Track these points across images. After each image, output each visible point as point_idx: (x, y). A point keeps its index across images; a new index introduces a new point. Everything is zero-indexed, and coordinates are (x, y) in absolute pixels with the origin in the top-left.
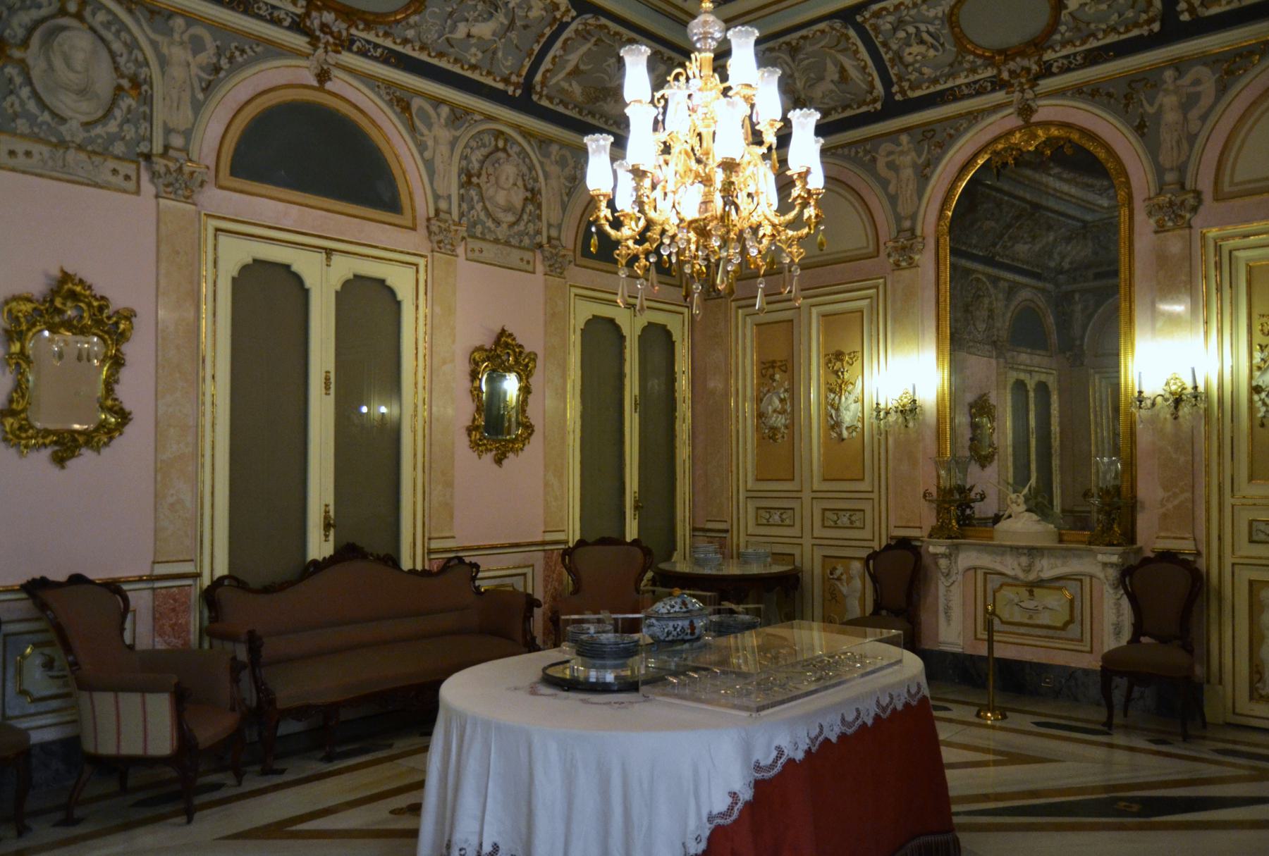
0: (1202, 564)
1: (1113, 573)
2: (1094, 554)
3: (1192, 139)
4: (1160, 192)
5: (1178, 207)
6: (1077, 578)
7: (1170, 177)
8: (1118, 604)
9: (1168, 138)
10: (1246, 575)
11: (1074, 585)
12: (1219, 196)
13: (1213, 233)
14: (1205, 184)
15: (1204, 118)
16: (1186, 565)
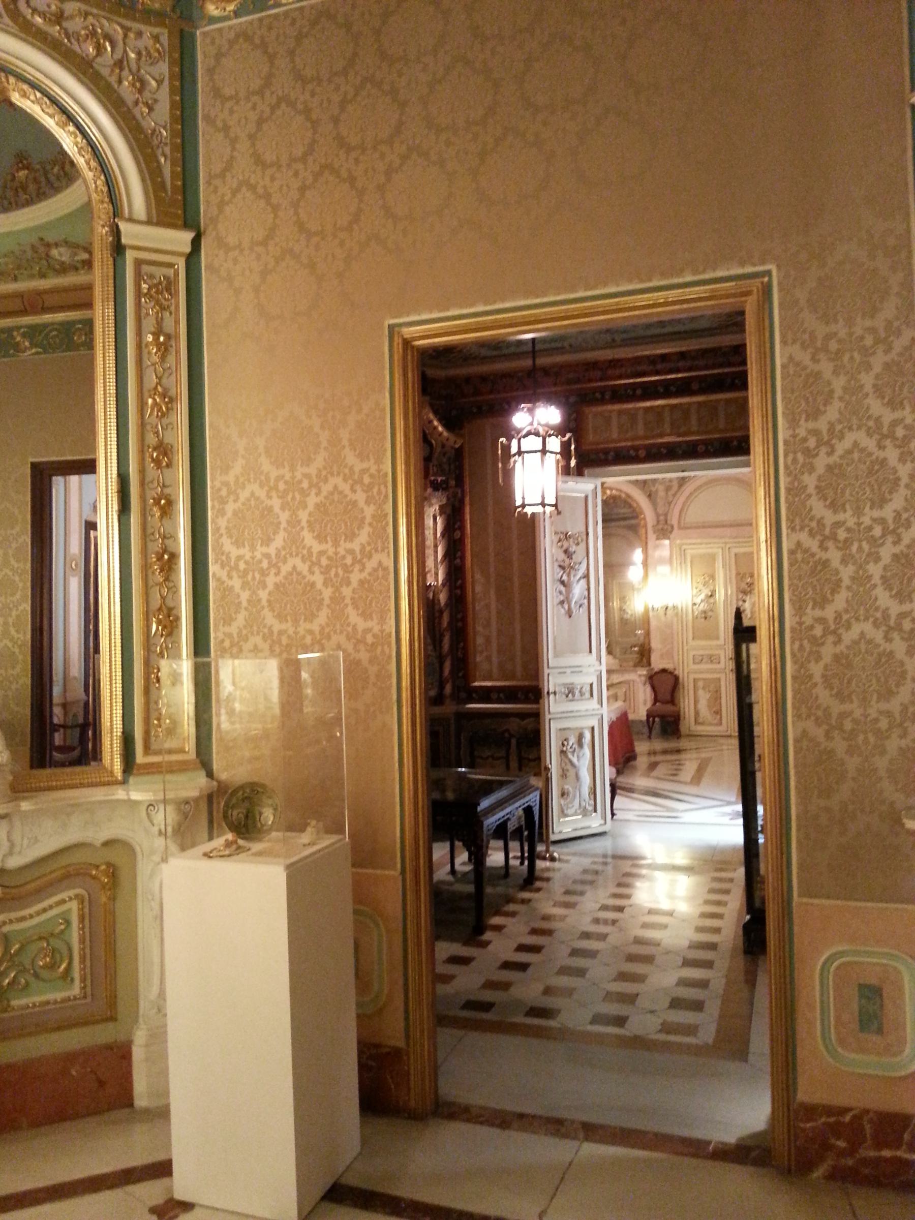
0: (676, 672)
1: (643, 679)
2: (636, 671)
3: (670, 503)
4: (658, 522)
5: (664, 531)
6: (627, 682)
7: (662, 518)
8: (645, 690)
9: (661, 502)
10: (692, 677)
11: (627, 686)
12: (680, 528)
13: (678, 542)
14: (674, 522)
15: (674, 495)
16: (671, 673)
